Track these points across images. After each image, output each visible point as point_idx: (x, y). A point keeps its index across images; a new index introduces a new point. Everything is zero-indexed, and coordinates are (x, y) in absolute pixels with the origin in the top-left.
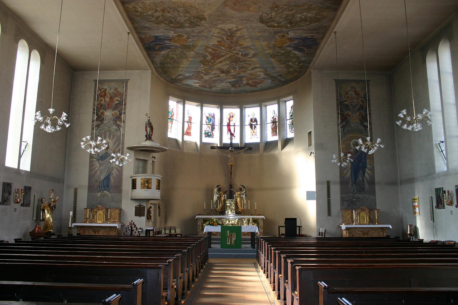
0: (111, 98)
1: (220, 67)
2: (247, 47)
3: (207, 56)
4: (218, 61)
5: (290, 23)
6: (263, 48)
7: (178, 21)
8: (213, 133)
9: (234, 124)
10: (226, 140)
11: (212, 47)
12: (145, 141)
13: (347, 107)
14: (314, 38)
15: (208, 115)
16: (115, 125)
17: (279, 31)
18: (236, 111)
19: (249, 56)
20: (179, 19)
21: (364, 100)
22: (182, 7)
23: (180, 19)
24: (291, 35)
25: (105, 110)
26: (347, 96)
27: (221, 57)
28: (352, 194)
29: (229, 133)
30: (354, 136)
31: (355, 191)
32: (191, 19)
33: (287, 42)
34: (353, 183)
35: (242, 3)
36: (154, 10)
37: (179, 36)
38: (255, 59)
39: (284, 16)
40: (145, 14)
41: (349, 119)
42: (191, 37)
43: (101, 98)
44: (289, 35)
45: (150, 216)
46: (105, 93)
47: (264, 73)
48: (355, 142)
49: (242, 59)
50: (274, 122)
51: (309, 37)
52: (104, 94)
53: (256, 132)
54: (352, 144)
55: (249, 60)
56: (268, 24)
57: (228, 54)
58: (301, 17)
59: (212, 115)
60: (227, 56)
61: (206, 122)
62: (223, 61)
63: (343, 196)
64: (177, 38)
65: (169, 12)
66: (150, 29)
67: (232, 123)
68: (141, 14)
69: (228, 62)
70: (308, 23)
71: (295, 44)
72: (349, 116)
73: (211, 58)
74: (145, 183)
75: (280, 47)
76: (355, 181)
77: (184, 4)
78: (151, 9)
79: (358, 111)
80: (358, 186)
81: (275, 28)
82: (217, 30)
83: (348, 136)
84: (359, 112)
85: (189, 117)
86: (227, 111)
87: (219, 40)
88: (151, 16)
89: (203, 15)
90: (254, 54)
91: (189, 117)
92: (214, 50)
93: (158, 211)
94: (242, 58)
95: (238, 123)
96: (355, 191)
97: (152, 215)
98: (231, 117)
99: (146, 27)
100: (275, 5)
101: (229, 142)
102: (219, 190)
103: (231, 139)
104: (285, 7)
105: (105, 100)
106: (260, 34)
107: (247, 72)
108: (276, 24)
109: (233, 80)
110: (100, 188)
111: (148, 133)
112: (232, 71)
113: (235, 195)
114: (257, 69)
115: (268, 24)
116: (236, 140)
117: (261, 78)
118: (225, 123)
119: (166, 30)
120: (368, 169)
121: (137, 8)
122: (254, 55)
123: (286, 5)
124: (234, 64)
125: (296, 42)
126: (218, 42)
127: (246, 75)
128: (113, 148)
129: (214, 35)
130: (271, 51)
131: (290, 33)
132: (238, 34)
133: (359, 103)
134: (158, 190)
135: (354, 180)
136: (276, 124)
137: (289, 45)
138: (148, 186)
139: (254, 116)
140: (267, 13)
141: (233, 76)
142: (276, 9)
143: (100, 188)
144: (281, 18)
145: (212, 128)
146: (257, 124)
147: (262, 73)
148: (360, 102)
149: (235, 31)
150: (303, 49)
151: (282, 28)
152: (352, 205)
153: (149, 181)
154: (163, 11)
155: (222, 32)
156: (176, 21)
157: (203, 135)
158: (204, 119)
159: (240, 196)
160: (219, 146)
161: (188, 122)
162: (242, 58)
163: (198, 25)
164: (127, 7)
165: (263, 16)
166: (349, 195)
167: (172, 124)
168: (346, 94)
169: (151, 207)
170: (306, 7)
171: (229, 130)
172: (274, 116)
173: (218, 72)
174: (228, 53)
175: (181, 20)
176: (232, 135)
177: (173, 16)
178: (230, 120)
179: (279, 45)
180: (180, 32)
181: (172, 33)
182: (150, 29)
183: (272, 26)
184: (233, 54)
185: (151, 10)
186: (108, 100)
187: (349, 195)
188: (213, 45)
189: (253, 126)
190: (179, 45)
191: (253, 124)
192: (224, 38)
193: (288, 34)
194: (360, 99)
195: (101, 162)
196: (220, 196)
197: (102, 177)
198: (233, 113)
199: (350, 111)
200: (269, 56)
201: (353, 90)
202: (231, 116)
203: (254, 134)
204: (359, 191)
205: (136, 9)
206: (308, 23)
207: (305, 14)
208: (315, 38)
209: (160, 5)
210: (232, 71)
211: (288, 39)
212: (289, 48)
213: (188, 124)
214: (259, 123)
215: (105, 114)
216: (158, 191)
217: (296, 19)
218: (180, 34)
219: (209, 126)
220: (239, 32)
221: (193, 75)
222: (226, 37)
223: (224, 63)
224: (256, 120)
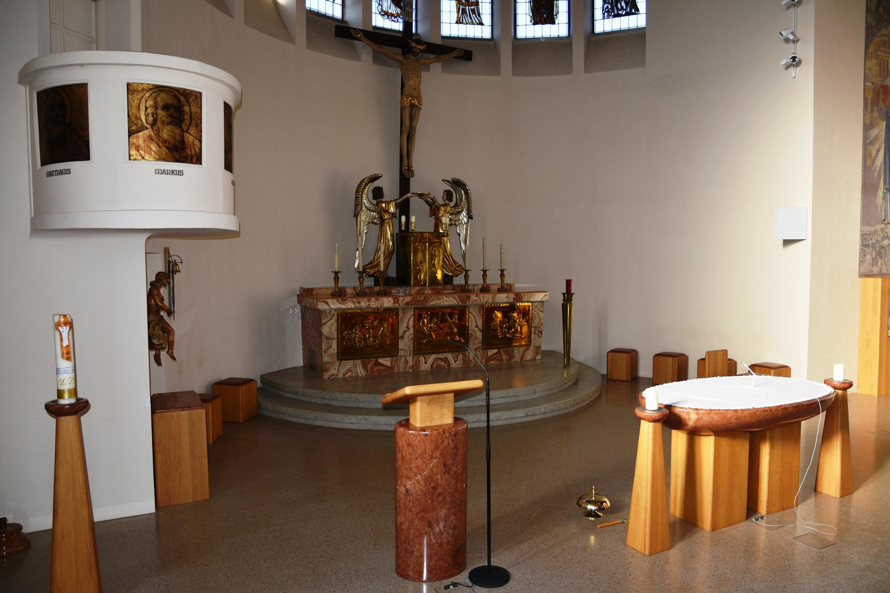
28: (883, 226)
34: (886, 189)
63: (868, 229)
74: (161, 112)
138: (182, 142)
153: (186, 109)
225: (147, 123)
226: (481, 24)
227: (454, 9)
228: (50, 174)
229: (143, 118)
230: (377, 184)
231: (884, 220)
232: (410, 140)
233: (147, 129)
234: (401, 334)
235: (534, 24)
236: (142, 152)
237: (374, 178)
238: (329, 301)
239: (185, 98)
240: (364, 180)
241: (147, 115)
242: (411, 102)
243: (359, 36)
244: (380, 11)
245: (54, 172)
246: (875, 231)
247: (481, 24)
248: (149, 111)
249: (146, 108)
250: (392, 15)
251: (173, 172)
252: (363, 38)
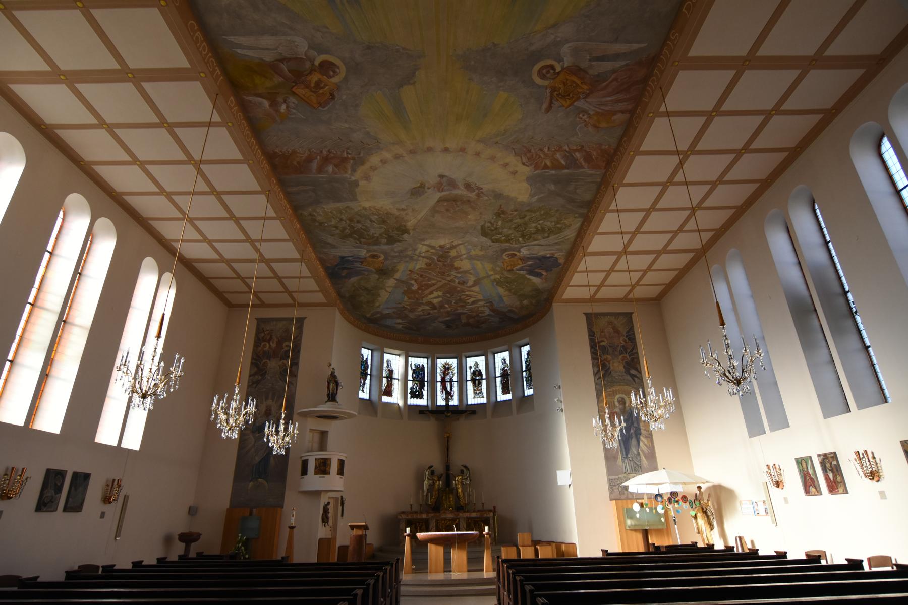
0: (279, 343)
1: (430, 300)
2: (466, 272)
3: (413, 285)
4: (427, 292)
5: (523, 236)
6: (487, 273)
7: (371, 234)
8: (422, 393)
9: (451, 379)
10: (441, 402)
11: (418, 272)
12: (326, 402)
13: (604, 350)
14: (555, 256)
15: (414, 368)
16: (282, 381)
17: (508, 247)
18: (454, 362)
19: (468, 285)
20: (372, 231)
21: (627, 339)
22: (376, 215)
23: (374, 232)
24: (523, 252)
25: (270, 360)
26: (603, 334)
27: (431, 287)
28: (625, 475)
29: (444, 392)
30: (619, 389)
31: (628, 470)
32: (389, 231)
33: (519, 264)
35: (458, 208)
36: (338, 219)
37: (374, 256)
38: (476, 289)
39: (513, 226)
40: (326, 225)
41: (609, 367)
42: (390, 258)
43: (264, 343)
44: (521, 253)
45: (328, 518)
46: (271, 336)
47: (489, 308)
48: (621, 397)
49: (459, 289)
50: (505, 375)
51: (548, 255)
52: (268, 337)
53: (481, 389)
54: (616, 401)
55: (468, 289)
56: (493, 238)
57: (440, 281)
58: (536, 227)
60: (440, 284)
61: (412, 376)
62: (434, 292)
63: (611, 477)
64: (371, 259)
65: (358, 222)
66: (333, 246)
67: (448, 378)
68: (321, 224)
69: (440, 294)
70: (546, 235)
71: (529, 266)
72: (609, 362)
73: (418, 288)
74: (321, 464)
75: (509, 271)
76: (627, 455)
77: (379, 210)
78: (334, 217)
79: (620, 355)
80: (632, 463)
81: (502, 242)
82: (424, 248)
83: (610, 390)
84: (622, 356)
85: (389, 370)
86: (440, 363)
87: (428, 261)
88: (334, 227)
89: (405, 226)
90: (475, 281)
91: (389, 370)
92: (421, 276)
93: (340, 508)
94: (459, 288)
95: (455, 378)
96: (628, 470)
97: (330, 515)
99: (328, 243)
100: (502, 211)
101: (443, 403)
102: (432, 473)
103: (447, 400)
104: (515, 213)
105: (270, 346)
106: (482, 253)
107: (467, 307)
108: (503, 238)
109: (447, 318)
110: (252, 475)
111: (331, 390)
112: (446, 306)
113: (454, 482)
114: (480, 303)
115: (493, 238)
116: (454, 402)
117: (487, 316)
118: (439, 378)
119: (355, 247)
120: (643, 437)
121: (315, 216)
122: (476, 283)
123: (516, 211)
124: (449, 296)
125: (530, 263)
126: (426, 264)
127: (465, 311)
128: (277, 413)
129: (421, 255)
130: (498, 276)
131: (522, 250)
132: (453, 253)
133: (621, 343)
134: (342, 477)
135: (624, 453)
136: (508, 378)
137: (522, 267)
139: (478, 367)
140: (491, 223)
141: (448, 312)
142: (502, 216)
143: (252, 475)
144: (510, 228)
145: (420, 384)
146: (482, 379)
147: (486, 308)
148: (622, 342)
149: (449, 248)
150: (540, 273)
151: (512, 244)
152: (625, 492)
154: (351, 220)
155: (431, 251)
156: (368, 235)
157: (409, 396)
158: (410, 372)
159: (462, 482)
160: (430, 409)
161: (387, 377)
162: (459, 288)
163: (399, 241)
164: (301, 214)
165: (486, 226)
166: (620, 476)
167: (365, 380)
168: (602, 332)
169: (329, 503)
170: (542, 212)
171: (444, 388)
172: (504, 367)
173: (428, 308)
174: (440, 279)
175: (375, 234)
176: (449, 395)
177: (363, 227)
179: (509, 268)
180: (375, 251)
181: (365, 252)
182: (333, 246)
183: (497, 241)
184: (446, 282)
185: (334, 218)
186: (274, 345)
187: (620, 476)
188: (420, 268)
189: (477, 382)
190: (373, 270)
191: (477, 378)
192: (434, 259)
193: (519, 251)
194: (621, 339)
195: (257, 435)
196: (433, 483)
197: (257, 459)
199: (609, 355)
200: (495, 283)
201: (610, 326)
203: (478, 391)
204: (633, 470)
205: (314, 218)
206: (546, 235)
207: (541, 222)
208: (555, 257)
209: (346, 211)
210: (446, 306)
211: (520, 259)
212: (522, 271)
213: (388, 380)
214: (484, 377)
215: (269, 364)
216: (341, 478)
217: (531, 230)
218: (376, 253)
219: (417, 382)
220: (454, 250)
221: (394, 312)
222: (437, 257)
223: (435, 294)
224: (480, 373)
226: (483, 397)
227: (473, 393)
228: (302, 478)
230: (432, 469)
231: (625, 472)
234: (430, 529)
235: (503, 394)
238: (402, 515)
246: (619, 478)
247: (483, 397)
251: (322, 477)
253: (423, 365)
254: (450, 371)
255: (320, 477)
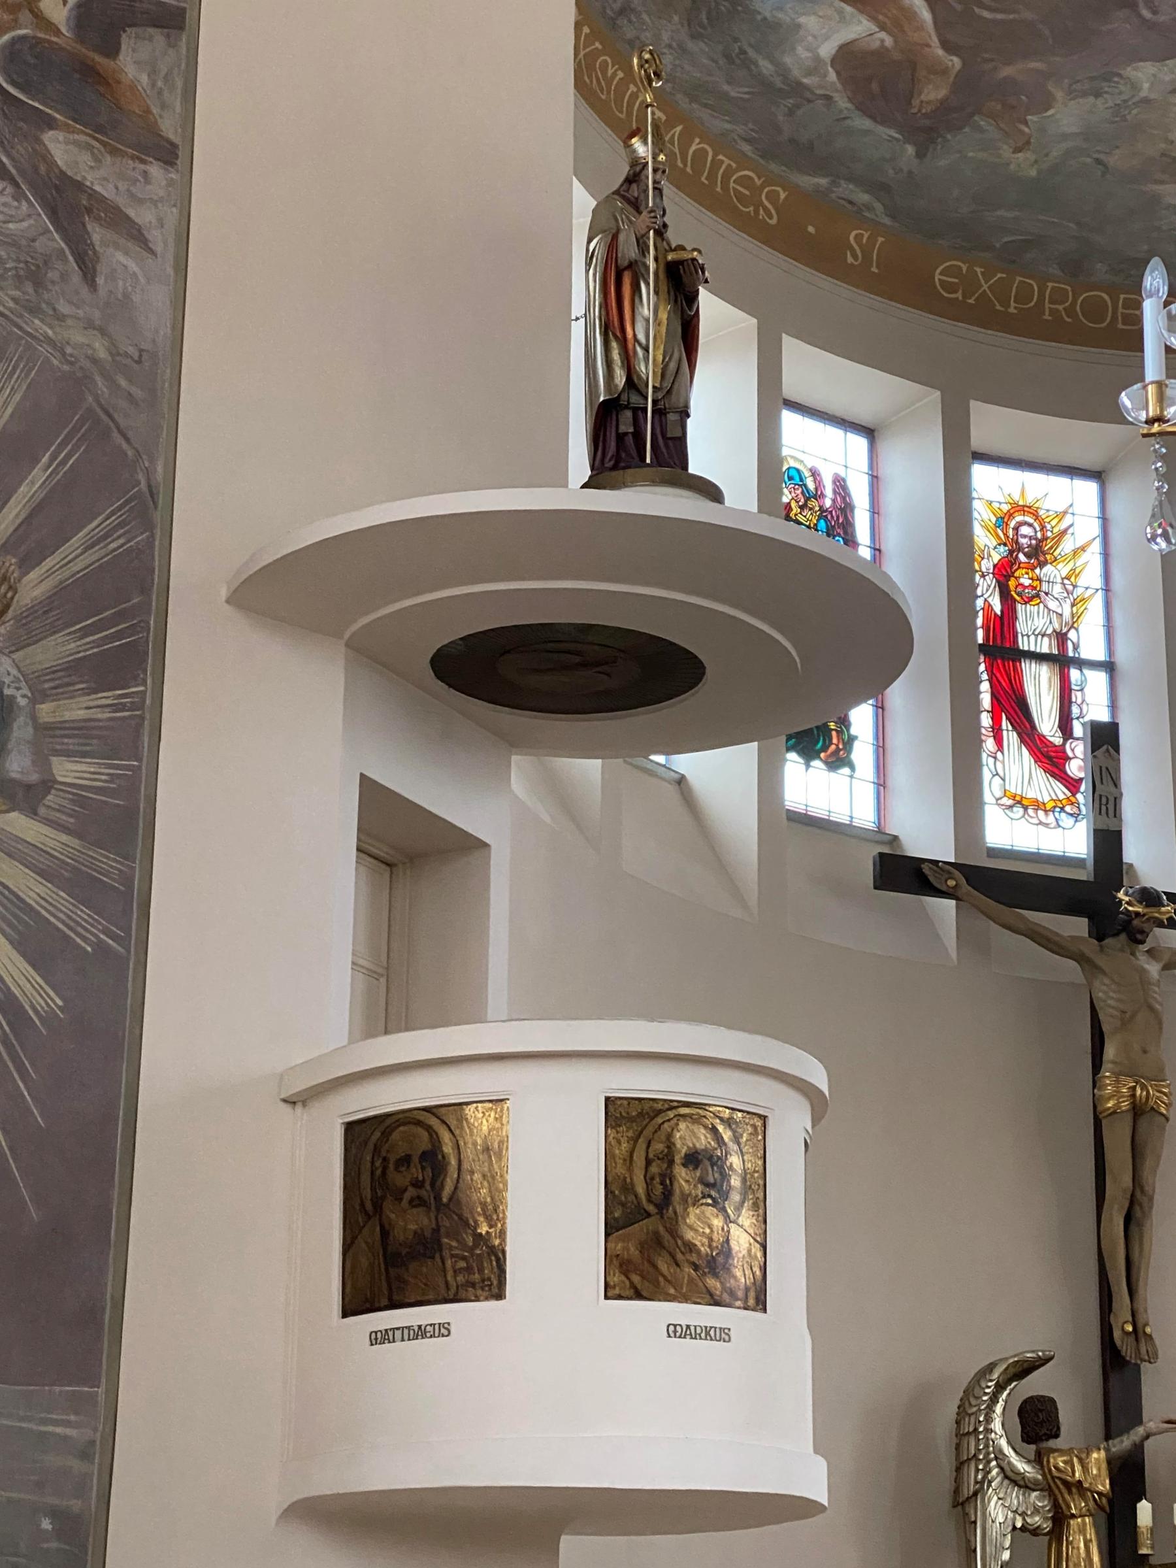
9: (1061, 638)
59: (828, 503)
98: (1022, 557)
178: (1012, 583)
198: (1036, 517)
202: (1024, 541)
225: (649, 1200)
229: (641, 1189)
230: (1034, 1385)
232: (1133, 1228)
233: (649, 1215)
236: (636, 1279)
237: (1023, 1369)
239: (734, 1132)
240: (991, 1367)
241: (649, 1180)
242: (1133, 1096)
243: (951, 883)
244: (998, 794)
245: (398, 1334)
248: (654, 1169)
249: (648, 1162)
250: (1038, 805)
251: (708, 1333)
252: (966, 888)
253: (840, 485)
254: (1048, 569)
255: (676, 1331)
